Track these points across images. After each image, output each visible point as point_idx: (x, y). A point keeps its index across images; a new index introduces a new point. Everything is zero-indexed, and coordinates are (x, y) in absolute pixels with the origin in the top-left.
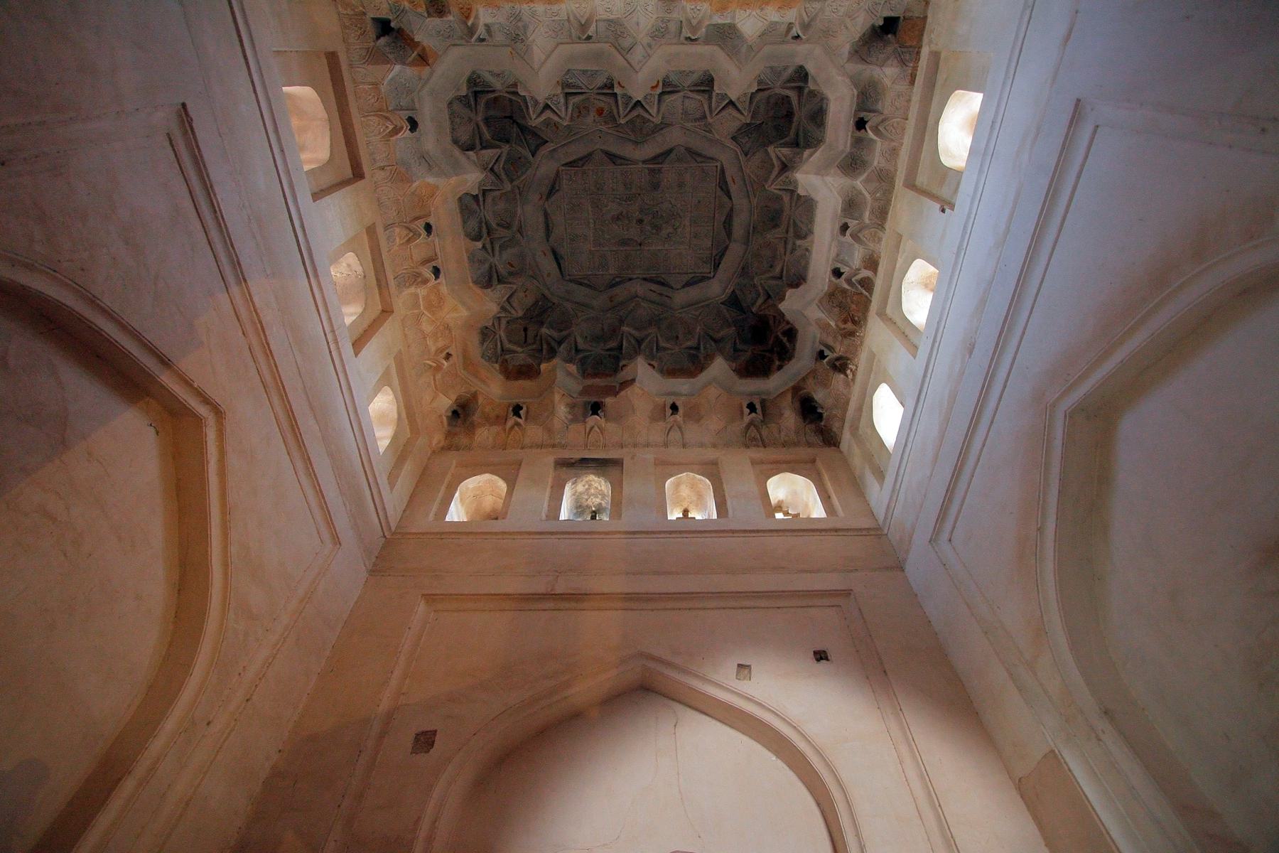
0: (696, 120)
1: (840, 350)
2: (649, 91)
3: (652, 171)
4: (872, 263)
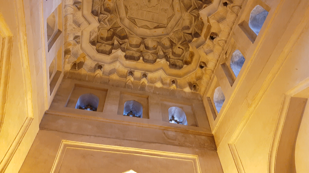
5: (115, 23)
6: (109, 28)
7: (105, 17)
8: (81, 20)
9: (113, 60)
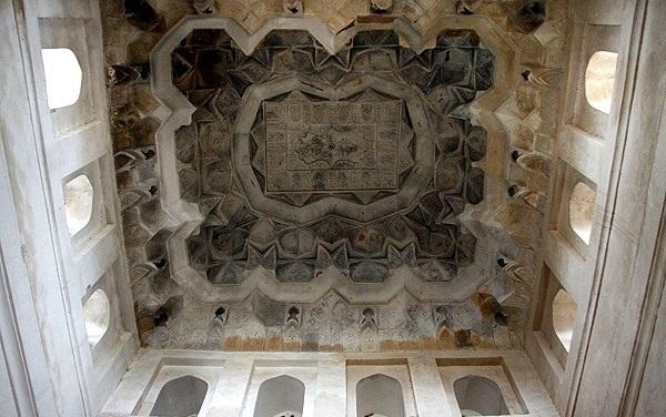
0: (287, 232)
2: (324, 271)
3: (321, 186)
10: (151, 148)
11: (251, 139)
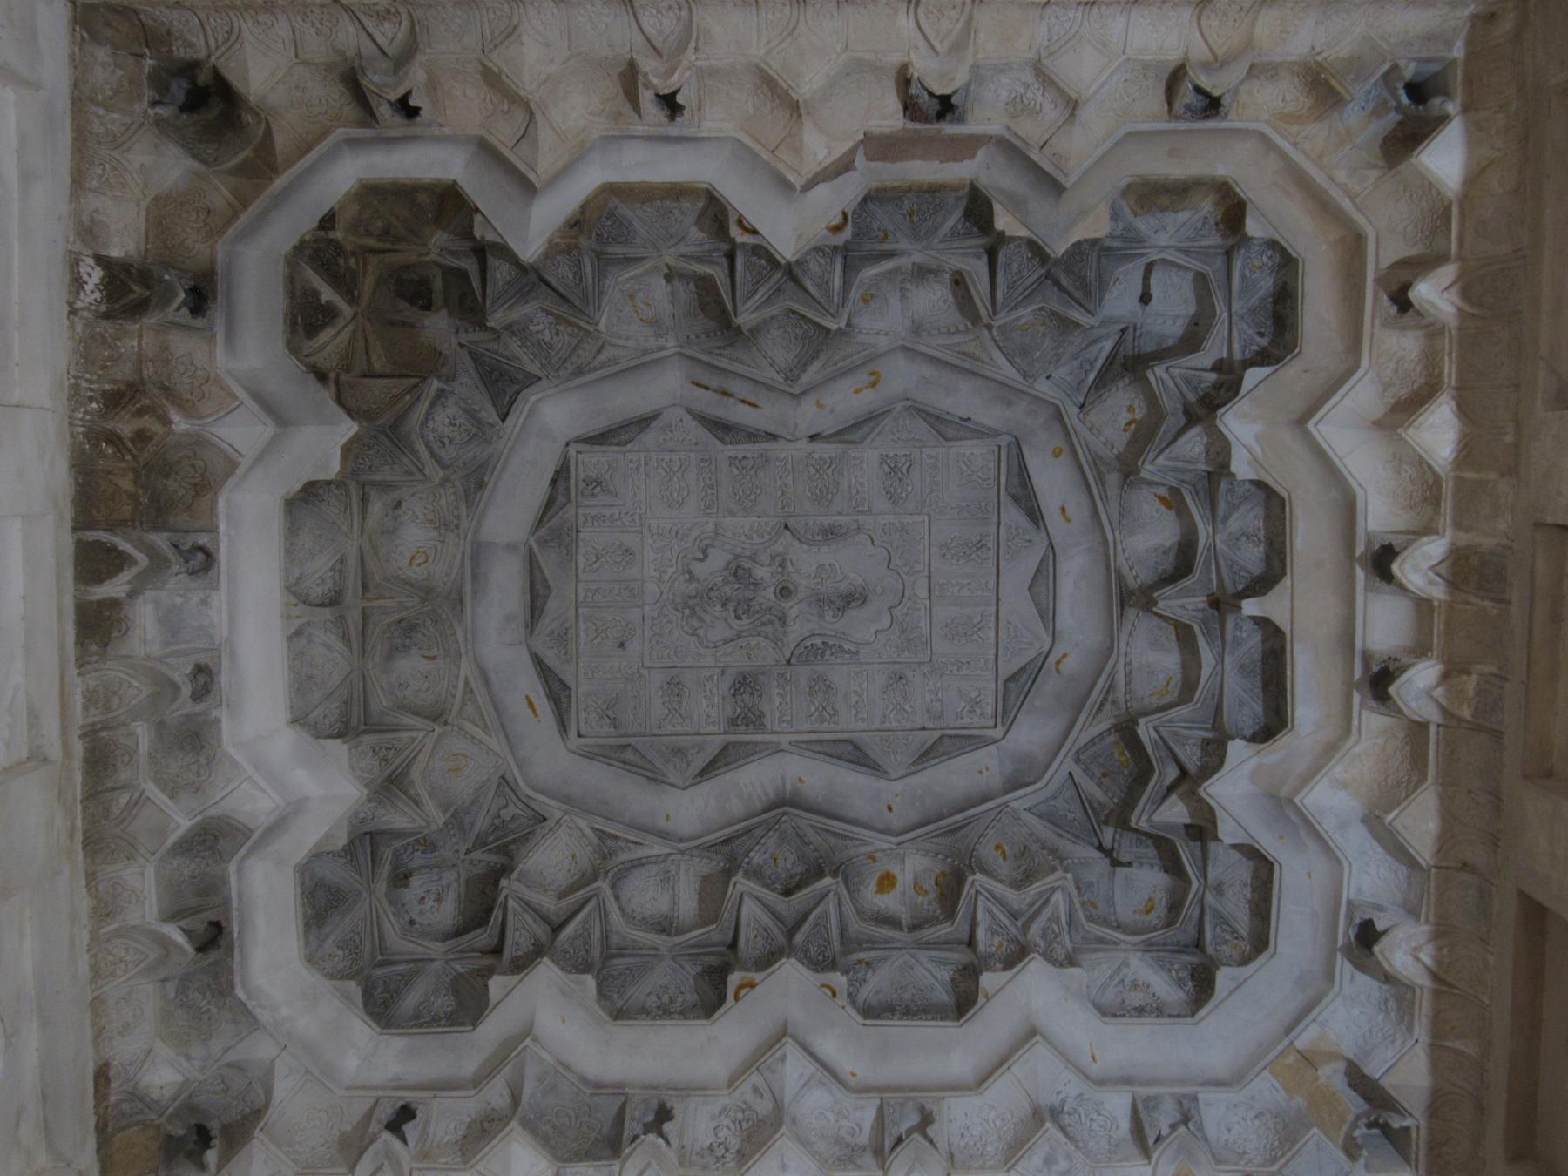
0: (639, 864)
1: (138, 339)
3: (750, 719)
4: (96, 626)
5: (1051, 818)
6: (1098, 854)
7: (990, 912)
8: (1001, 1103)
9: (1302, 833)
10: (203, 540)
11: (532, 564)
